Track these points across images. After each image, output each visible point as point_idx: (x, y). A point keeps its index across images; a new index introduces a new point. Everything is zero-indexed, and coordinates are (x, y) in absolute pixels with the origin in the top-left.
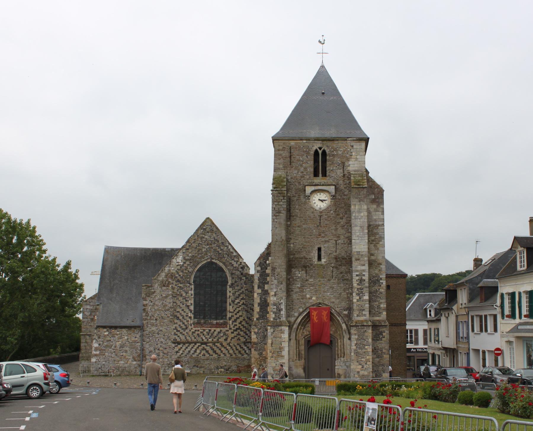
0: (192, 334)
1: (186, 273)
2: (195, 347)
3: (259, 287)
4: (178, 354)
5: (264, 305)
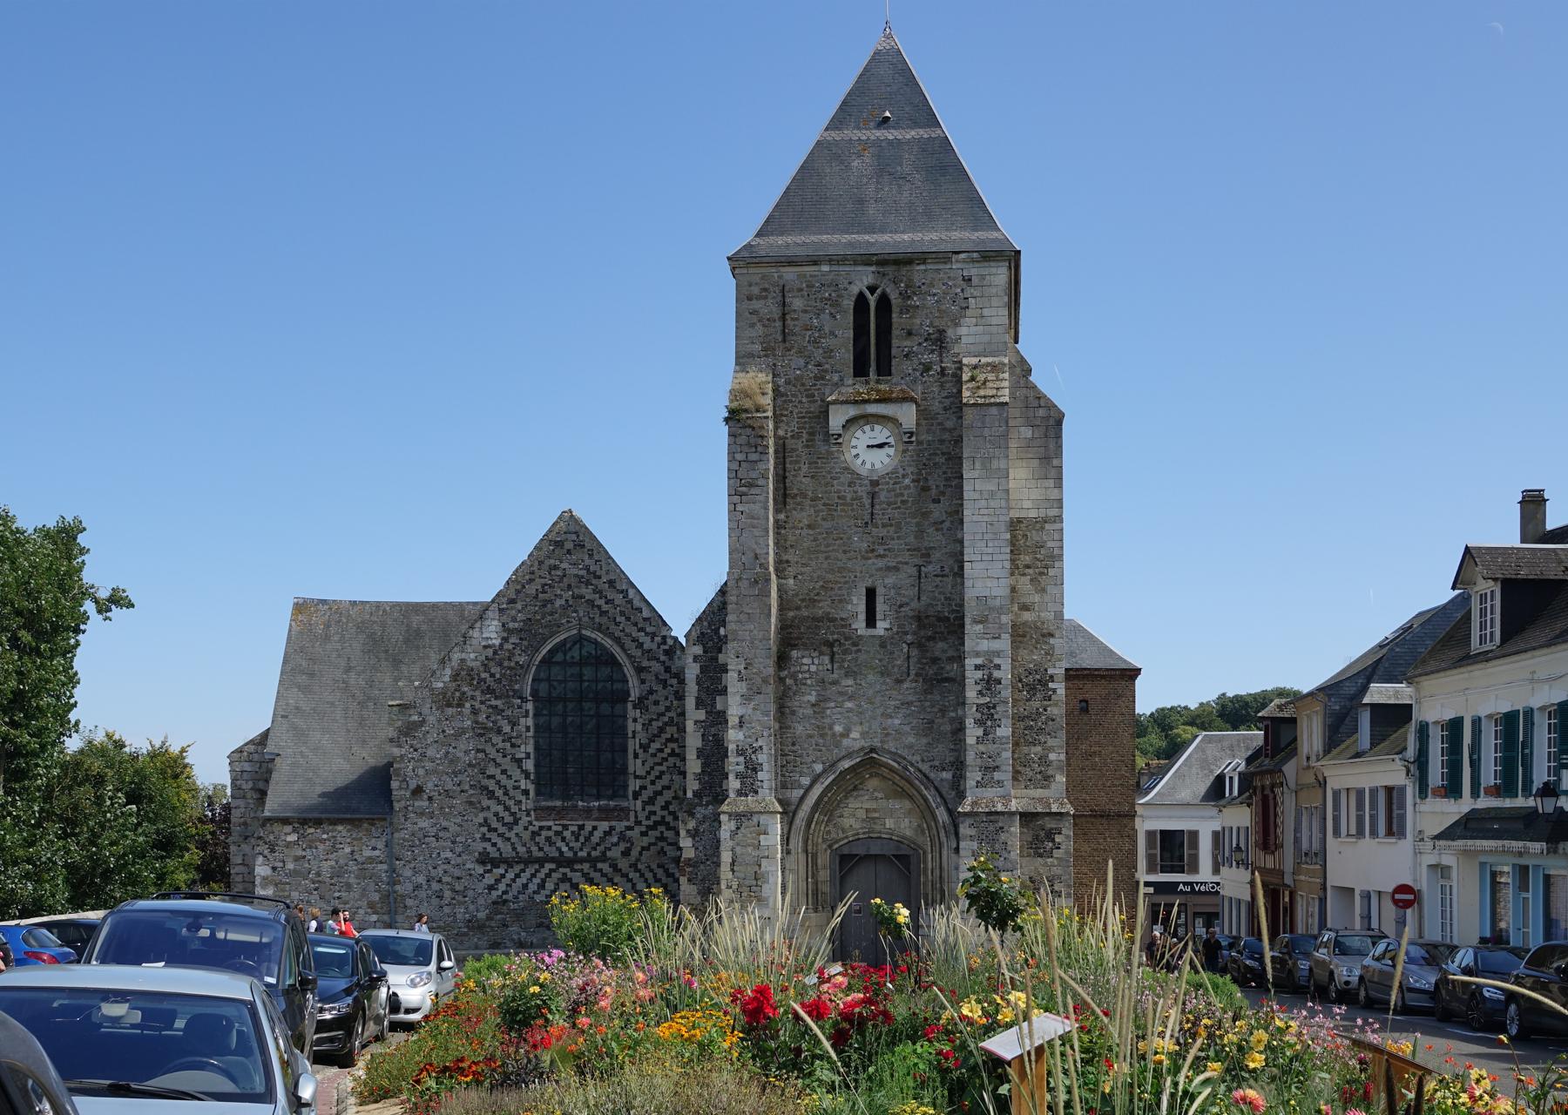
0: (533, 838)
1: (510, 668)
2: (541, 875)
3: (699, 704)
4: (495, 894)
5: (714, 753)
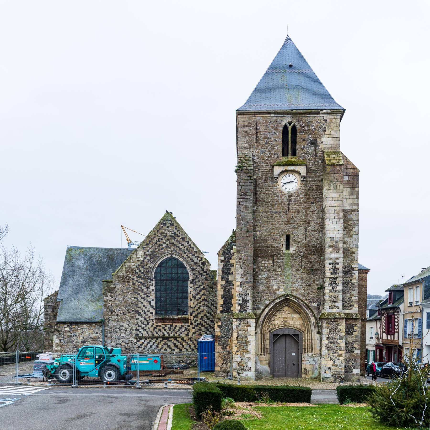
1: (146, 268)
3: (223, 278)
5: (228, 297)
